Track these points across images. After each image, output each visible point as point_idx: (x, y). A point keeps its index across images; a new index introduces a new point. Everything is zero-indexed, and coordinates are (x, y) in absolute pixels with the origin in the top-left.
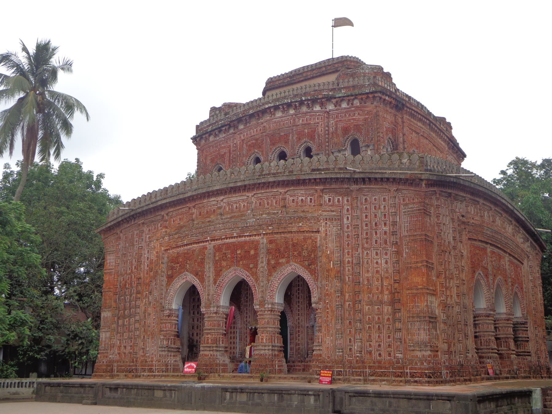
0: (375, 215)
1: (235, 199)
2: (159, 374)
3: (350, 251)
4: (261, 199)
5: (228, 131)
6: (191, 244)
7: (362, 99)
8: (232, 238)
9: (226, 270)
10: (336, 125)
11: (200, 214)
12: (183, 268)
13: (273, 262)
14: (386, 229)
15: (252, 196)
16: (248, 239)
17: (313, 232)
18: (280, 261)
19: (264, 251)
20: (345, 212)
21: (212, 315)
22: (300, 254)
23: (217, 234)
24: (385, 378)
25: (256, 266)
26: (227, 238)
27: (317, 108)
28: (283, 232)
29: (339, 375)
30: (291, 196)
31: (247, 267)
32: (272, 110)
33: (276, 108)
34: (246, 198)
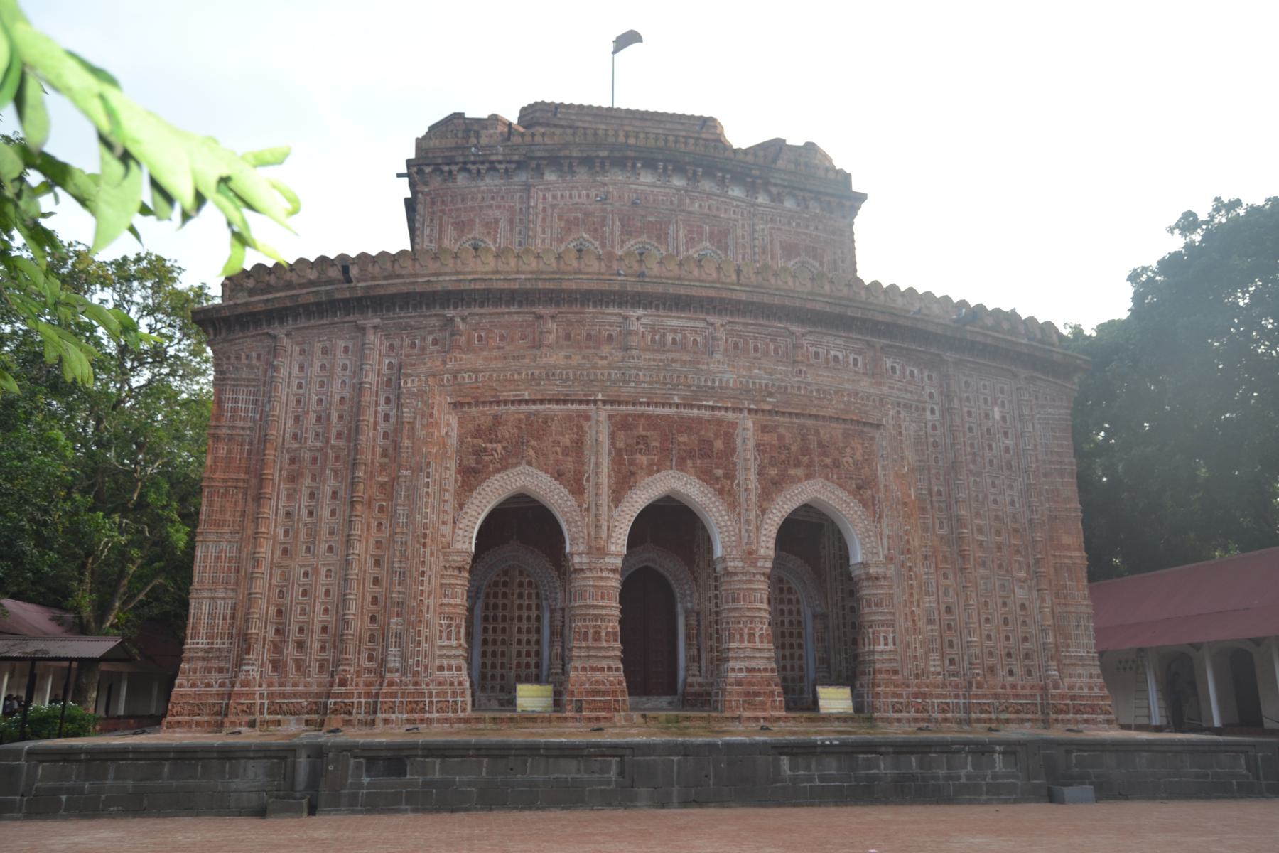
0: (987, 416)
1: (675, 322)
2: (445, 715)
3: (942, 473)
4: (740, 337)
5: (510, 177)
6: (542, 402)
8: (664, 405)
9: (650, 474)
10: (771, 235)
11: (568, 337)
13: (773, 472)
14: (1009, 442)
16: (707, 414)
17: (865, 424)
18: (792, 472)
19: (751, 444)
20: (926, 398)
21: (605, 574)
22: (837, 464)
23: (626, 391)
24: (1030, 716)
25: (730, 476)
26: (648, 404)
27: (736, 192)
29: (944, 711)
30: (813, 345)
31: (706, 476)
33: (650, 164)
34: (702, 325)
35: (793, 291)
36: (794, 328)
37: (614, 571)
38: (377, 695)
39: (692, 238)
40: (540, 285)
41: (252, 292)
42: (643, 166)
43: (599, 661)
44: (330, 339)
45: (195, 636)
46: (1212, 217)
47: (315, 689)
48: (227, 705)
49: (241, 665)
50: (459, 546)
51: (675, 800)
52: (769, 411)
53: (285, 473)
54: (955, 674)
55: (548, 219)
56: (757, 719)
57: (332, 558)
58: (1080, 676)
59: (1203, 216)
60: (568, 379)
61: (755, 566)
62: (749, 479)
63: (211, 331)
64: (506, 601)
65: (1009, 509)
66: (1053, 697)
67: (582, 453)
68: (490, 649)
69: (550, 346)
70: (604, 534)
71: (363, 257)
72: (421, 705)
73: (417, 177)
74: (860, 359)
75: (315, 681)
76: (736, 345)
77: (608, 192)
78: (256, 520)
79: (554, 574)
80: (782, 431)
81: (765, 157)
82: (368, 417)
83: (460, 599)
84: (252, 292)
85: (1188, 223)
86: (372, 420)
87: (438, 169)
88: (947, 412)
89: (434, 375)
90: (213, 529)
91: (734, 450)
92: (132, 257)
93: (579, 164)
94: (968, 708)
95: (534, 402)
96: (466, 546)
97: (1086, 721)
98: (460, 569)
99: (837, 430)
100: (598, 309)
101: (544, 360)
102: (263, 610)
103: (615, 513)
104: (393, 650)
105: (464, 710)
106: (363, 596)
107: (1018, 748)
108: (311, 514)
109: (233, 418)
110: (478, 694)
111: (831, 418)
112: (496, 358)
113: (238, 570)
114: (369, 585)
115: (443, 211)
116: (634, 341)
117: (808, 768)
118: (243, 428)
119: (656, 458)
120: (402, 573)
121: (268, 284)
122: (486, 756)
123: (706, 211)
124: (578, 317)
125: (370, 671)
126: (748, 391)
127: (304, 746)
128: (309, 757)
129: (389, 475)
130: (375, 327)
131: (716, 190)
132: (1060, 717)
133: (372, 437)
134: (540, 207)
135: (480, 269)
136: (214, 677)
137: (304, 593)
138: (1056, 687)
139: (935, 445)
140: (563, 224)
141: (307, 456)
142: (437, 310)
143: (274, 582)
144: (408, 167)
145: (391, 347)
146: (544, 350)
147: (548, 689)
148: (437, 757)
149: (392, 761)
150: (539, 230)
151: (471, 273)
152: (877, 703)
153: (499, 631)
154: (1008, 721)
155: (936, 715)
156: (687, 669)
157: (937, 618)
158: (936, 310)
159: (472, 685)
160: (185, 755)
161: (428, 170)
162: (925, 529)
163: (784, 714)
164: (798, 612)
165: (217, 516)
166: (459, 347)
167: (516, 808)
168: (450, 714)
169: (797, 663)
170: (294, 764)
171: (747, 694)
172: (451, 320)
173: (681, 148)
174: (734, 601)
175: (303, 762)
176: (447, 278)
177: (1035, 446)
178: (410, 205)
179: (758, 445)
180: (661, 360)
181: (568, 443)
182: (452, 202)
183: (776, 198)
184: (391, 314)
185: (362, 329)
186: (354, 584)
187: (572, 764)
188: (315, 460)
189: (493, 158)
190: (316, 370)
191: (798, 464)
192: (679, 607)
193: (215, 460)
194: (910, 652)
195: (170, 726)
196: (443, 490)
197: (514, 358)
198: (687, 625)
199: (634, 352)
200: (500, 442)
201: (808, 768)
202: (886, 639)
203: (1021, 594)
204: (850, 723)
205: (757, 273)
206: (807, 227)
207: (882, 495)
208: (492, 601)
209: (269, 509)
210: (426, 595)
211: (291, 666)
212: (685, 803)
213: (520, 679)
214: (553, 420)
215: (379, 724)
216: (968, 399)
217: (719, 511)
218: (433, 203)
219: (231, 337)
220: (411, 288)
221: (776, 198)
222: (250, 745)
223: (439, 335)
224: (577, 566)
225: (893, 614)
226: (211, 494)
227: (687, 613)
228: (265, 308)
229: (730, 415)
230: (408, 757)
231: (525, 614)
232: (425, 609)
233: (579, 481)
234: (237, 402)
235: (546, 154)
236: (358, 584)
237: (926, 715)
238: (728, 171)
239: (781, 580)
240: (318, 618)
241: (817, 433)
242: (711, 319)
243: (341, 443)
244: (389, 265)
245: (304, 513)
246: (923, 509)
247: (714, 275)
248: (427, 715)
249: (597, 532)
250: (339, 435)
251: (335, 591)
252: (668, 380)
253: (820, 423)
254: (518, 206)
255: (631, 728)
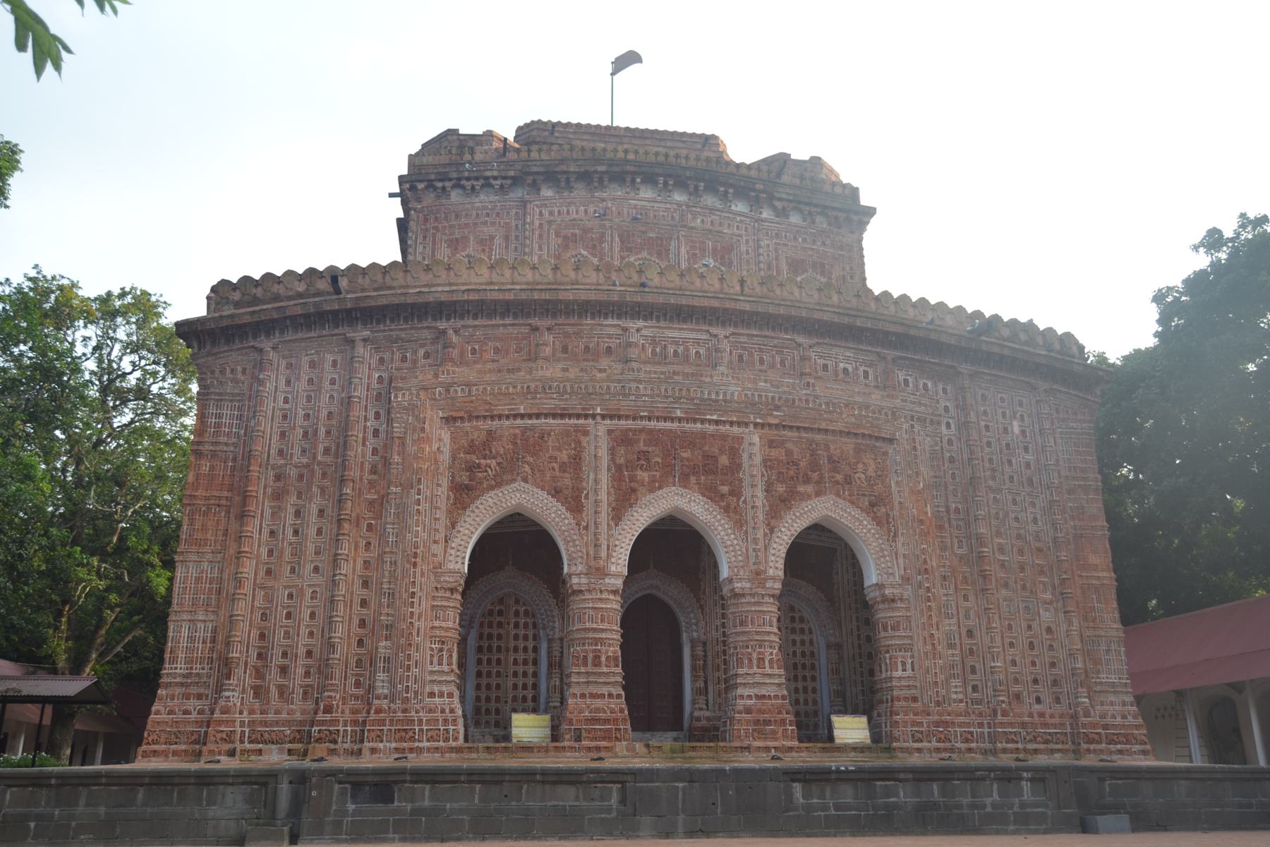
0: (1006, 430)
1: (676, 334)
2: (436, 744)
3: (960, 490)
4: (745, 349)
6: (538, 416)
7: (836, 218)
8: (665, 419)
9: (652, 491)
11: (565, 349)
12: (507, 473)
13: (781, 489)
15: (726, 337)
16: (711, 428)
17: (877, 438)
18: (801, 489)
19: (758, 460)
22: (848, 481)
24: (1059, 746)
25: (736, 493)
27: (740, 207)
28: (805, 428)
29: (967, 741)
31: (711, 493)
32: (638, 180)
33: (650, 180)
35: (799, 302)
36: (801, 339)
37: (615, 592)
38: (364, 722)
39: (695, 254)
40: (536, 296)
41: (237, 305)
42: (642, 182)
43: (599, 689)
44: (318, 353)
45: (174, 660)
46: (1238, 234)
47: (298, 716)
48: (206, 733)
49: (221, 691)
50: (451, 566)
51: (680, 830)
52: (776, 425)
53: (269, 490)
54: (979, 702)
55: (545, 236)
56: (767, 749)
57: (318, 579)
58: (1112, 704)
59: (1228, 233)
60: (565, 392)
61: (764, 587)
62: (755, 496)
63: (196, 346)
64: (501, 631)
65: (1032, 527)
66: (1084, 726)
67: (580, 469)
68: (484, 681)
69: (546, 359)
70: (604, 554)
71: (353, 268)
72: (411, 734)
73: (409, 194)
74: (871, 371)
75: (298, 708)
76: (741, 356)
77: (607, 208)
78: (239, 539)
79: (553, 601)
80: (789, 445)
81: (769, 172)
82: (357, 432)
83: (451, 621)
84: (237, 305)
85: (1213, 240)
86: (361, 436)
87: (430, 186)
88: (964, 425)
89: (426, 389)
90: (194, 549)
91: (740, 466)
92: (116, 292)
93: (577, 179)
94: (993, 738)
95: (530, 416)
96: (458, 566)
97: (1120, 752)
98: (452, 590)
99: (849, 445)
100: (597, 321)
101: (541, 373)
102: (245, 633)
103: (615, 532)
104: (381, 676)
105: (456, 739)
106: (350, 619)
107: (1047, 775)
108: (296, 532)
109: (216, 434)
110: (471, 729)
111: (841, 432)
112: (490, 371)
113: (219, 592)
114: (356, 608)
115: (436, 228)
116: (634, 353)
117: (822, 796)
118: (226, 444)
119: (658, 474)
120: (391, 595)
121: (255, 297)
122: (479, 782)
123: (708, 226)
124: (575, 329)
125: (357, 698)
126: (753, 404)
127: (286, 771)
128: (291, 782)
129: (377, 492)
130: (364, 340)
131: (718, 205)
132: (1092, 747)
133: (361, 453)
134: (537, 223)
135: (473, 278)
136: (192, 704)
137: (289, 616)
138: (1087, 714)
139: (952, 460)
140: (560, 241)
141: (293, 472)
142: (429, 322)
143: (257, 604)
144: (400, 184)
145: (382, 361)
146: (540, 362)
147: (544, 719)
148: (427, 782)
149: (379, 787)
150: (536, 246)
151: (464, 284)
152: (896, 733)
153: (494, 663)
154: (1036, 751)
155: (959, 745)
156: (694, 702)
157: (957, 641)
158: (949, 321)
159: (464, 716)
160: (160, 780)
161: (421, 186)
162: (944, 549)
163: (796, 743)
164: (811, 642)
165: (198, 536)
166: (452, 360)
167: (511, 838)
168: (441, 744)
169: (810, 696)
170: (276, 789)
171: (757, 722)
172: (444, 332)
173: (684, 165)
174: (741, 625)
175: (284, 789)
176: (440, 289)
177: (1057, 461)
178: (402, 225)
179: (765, 461)
180: (662, 373)
181: (565, 459)
182: (446, 218)
183: (782, 213)
184: (382, 327)
185: (351, 342)
186: (341, 606)
187: (571, 791)
188: (301, 476)
189: (488, 174)
190: (302, 385)
191: (807, 481)
192: (685, 635)
193: (197, 477)
194: (930, 678)
195: (146, 755)
196: (434, 507)
197: (509, 371)
198: (694, 657)
199: (633, 364)
200: (494, 458)
201: (822, 796)
202: (904, 664)
203: (1046, 616)
204: (867, 754)
205: (762, 284)
206: (814, 242)
207: (896, 513)
208: (486, 631)
209: (252, 527)
210: (416, 617)
211: (274, 692)
212: (691, 833)
213: (515, 711)
214: (549, 435)
215: (366, 752)
216: (985, 413)
217: (725, 530)
218: (426, 220)
219: (216, 350)
220: (402, 300)
221: (782, 213)
222: (228, 771)
223: (429, 348)
224: (575, 588)
225: (911, 638)
226: (192, 513)
227: (693, 643)
228: (251, 319)
229: (735, 429)
230: (395, 782)
231: (521, 644)
232: (415, 633)
233: (577, 499)
234: (221, 417)
235: (542, 169)
236: (345, 606)
237: (948, 745)
238: (731, 186)
239: (792, 609)
240: (303, 642)
241: (827, 448)
242: (714, 330)
243: (328, 459)
244: (379, 277)
245: (289, 532)
246: (941, 528)
247: (717, 285)
248: (417, 744)
249: (596, 552)
250: (327, 451)
251: (320, 613)
252: (670, 393)
253: (830, 437)
254: (513, 224)
255: (630, 754)
